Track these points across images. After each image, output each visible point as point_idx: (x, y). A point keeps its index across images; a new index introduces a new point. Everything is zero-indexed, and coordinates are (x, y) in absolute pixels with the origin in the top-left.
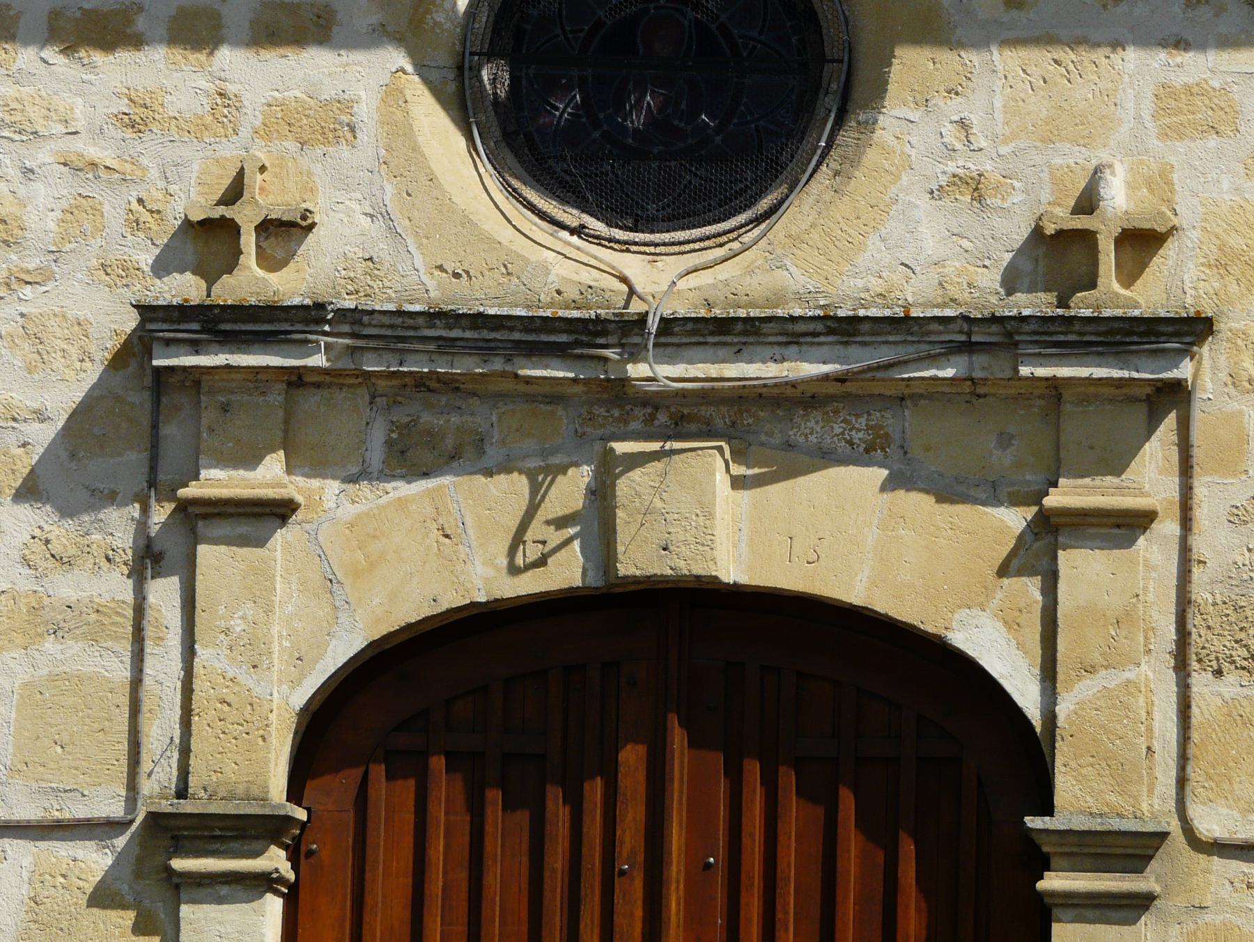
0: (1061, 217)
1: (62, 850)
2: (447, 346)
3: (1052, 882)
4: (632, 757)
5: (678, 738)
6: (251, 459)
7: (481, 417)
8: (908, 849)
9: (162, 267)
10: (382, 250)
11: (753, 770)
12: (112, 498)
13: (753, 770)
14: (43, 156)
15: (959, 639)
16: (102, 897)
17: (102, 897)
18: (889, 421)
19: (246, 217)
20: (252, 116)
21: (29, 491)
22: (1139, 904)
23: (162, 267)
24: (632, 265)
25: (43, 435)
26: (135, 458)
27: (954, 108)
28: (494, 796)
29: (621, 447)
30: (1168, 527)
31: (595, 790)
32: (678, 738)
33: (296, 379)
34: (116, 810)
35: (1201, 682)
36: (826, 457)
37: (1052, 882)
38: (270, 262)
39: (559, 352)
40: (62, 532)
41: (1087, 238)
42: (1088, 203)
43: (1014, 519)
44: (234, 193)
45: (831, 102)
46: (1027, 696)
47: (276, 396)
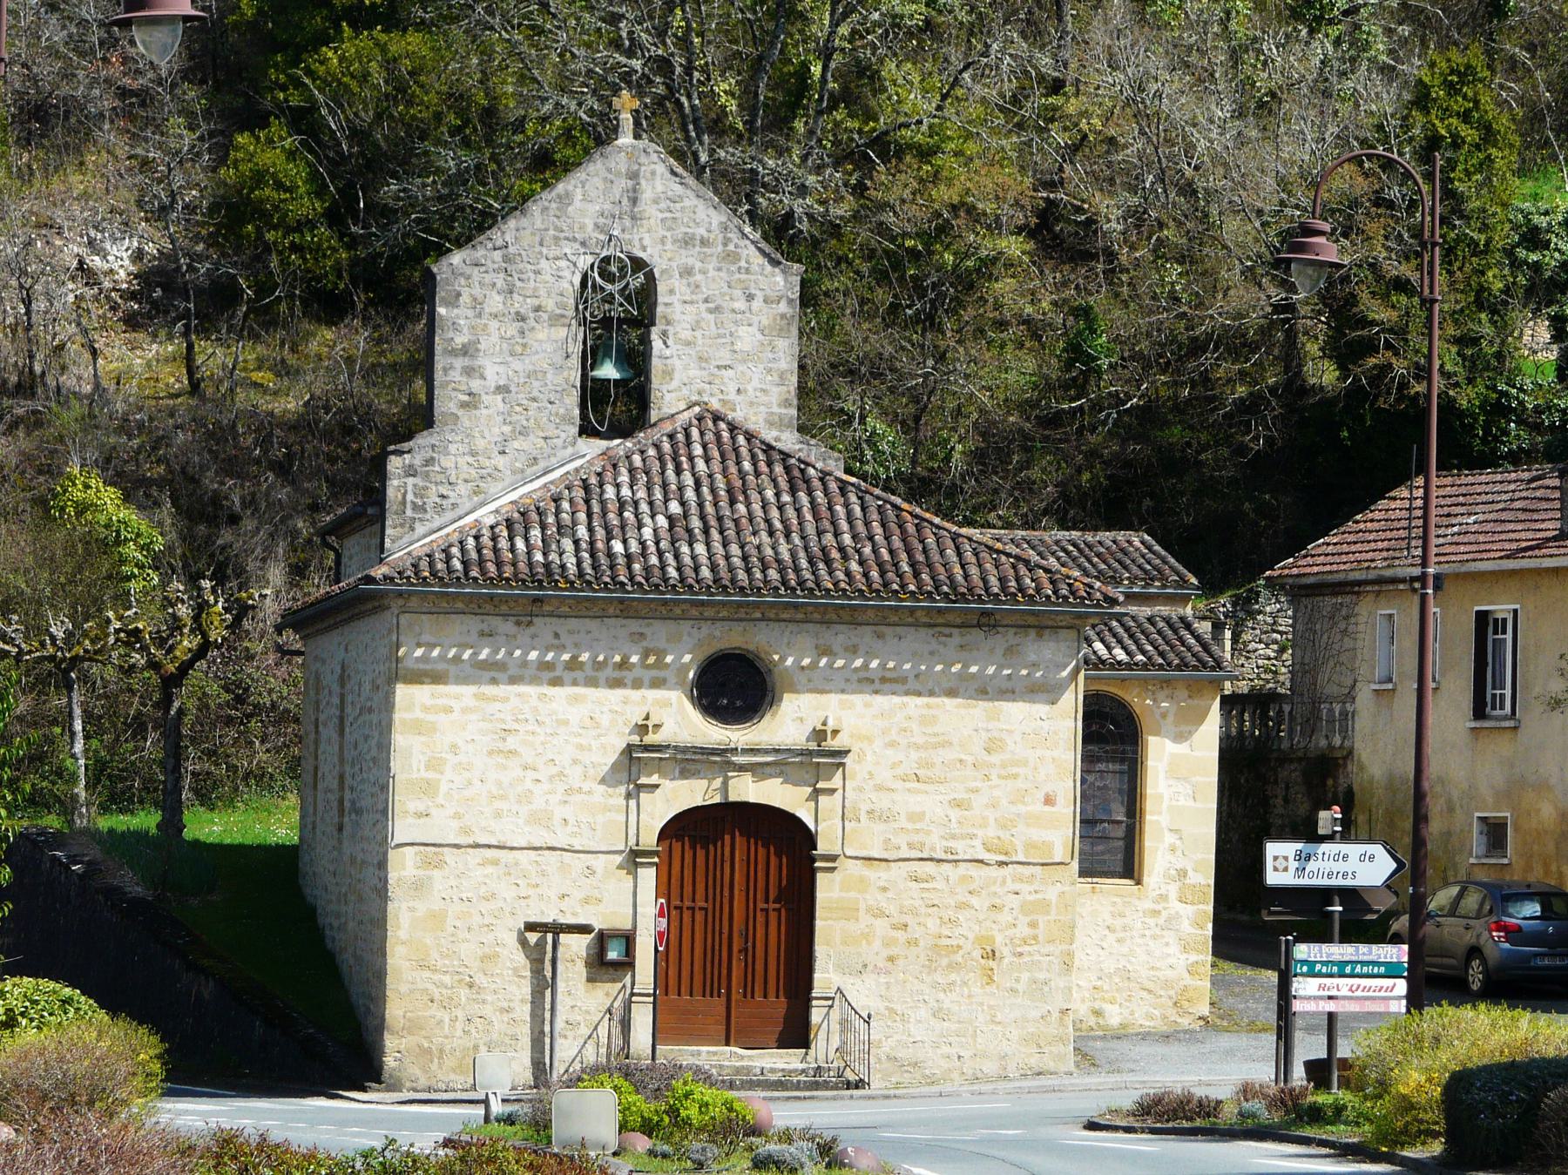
0: (819, 727)
1: (611, 857)
2: (695, 753)
3: (817, 864)
4: (727, 838)
5: (737, 834)
6: (650, 775)
7: (699, 766)
8: (784, 860)
9: (630, 734)
10: (678, 731)
11: (752, 841)
12: (621, 783)
13: (752, 841)
14: (605, 709)
15: (798, 814)
16: (620, 867)
17: (620, 867)
18: (783, 768)
19: (650, 723)
20: (650, 700)
21: (603, 781)
22: (834, 869)
23: (630, 734)
24: (728, 733)
25: (606, 768)
26: (626, 774)
27: (797, 703)
28: (698, 846)
29: (730, 774)
30: (840, 791)
31: (719, 844)
32: (737, 834)
33: (661, 759)
34: (622, 848)
35: (846, 823)
36: (771, 776)
37: (817, 864)
38: (654, 733)
39: (718, 755)
40: (610, 790)
41: (825, 731)
42: (824, 724)
43: (810, 790)
44: (647, 718)
45: (769, 699)
46: (812, 827)
47: (656, 762)
